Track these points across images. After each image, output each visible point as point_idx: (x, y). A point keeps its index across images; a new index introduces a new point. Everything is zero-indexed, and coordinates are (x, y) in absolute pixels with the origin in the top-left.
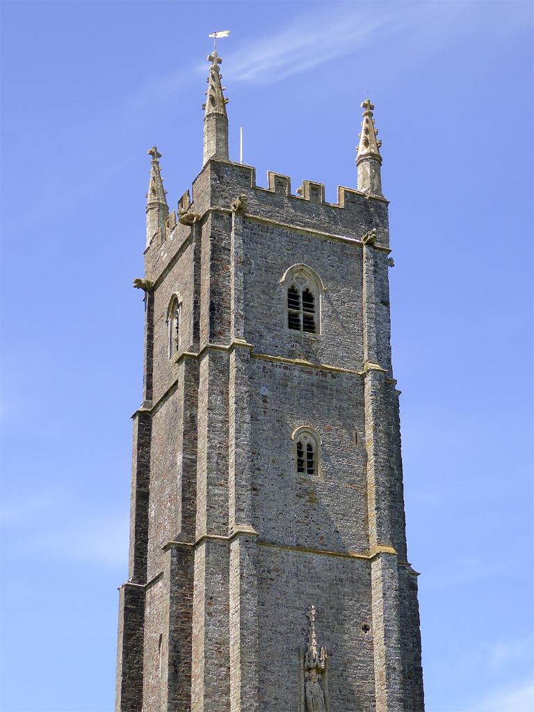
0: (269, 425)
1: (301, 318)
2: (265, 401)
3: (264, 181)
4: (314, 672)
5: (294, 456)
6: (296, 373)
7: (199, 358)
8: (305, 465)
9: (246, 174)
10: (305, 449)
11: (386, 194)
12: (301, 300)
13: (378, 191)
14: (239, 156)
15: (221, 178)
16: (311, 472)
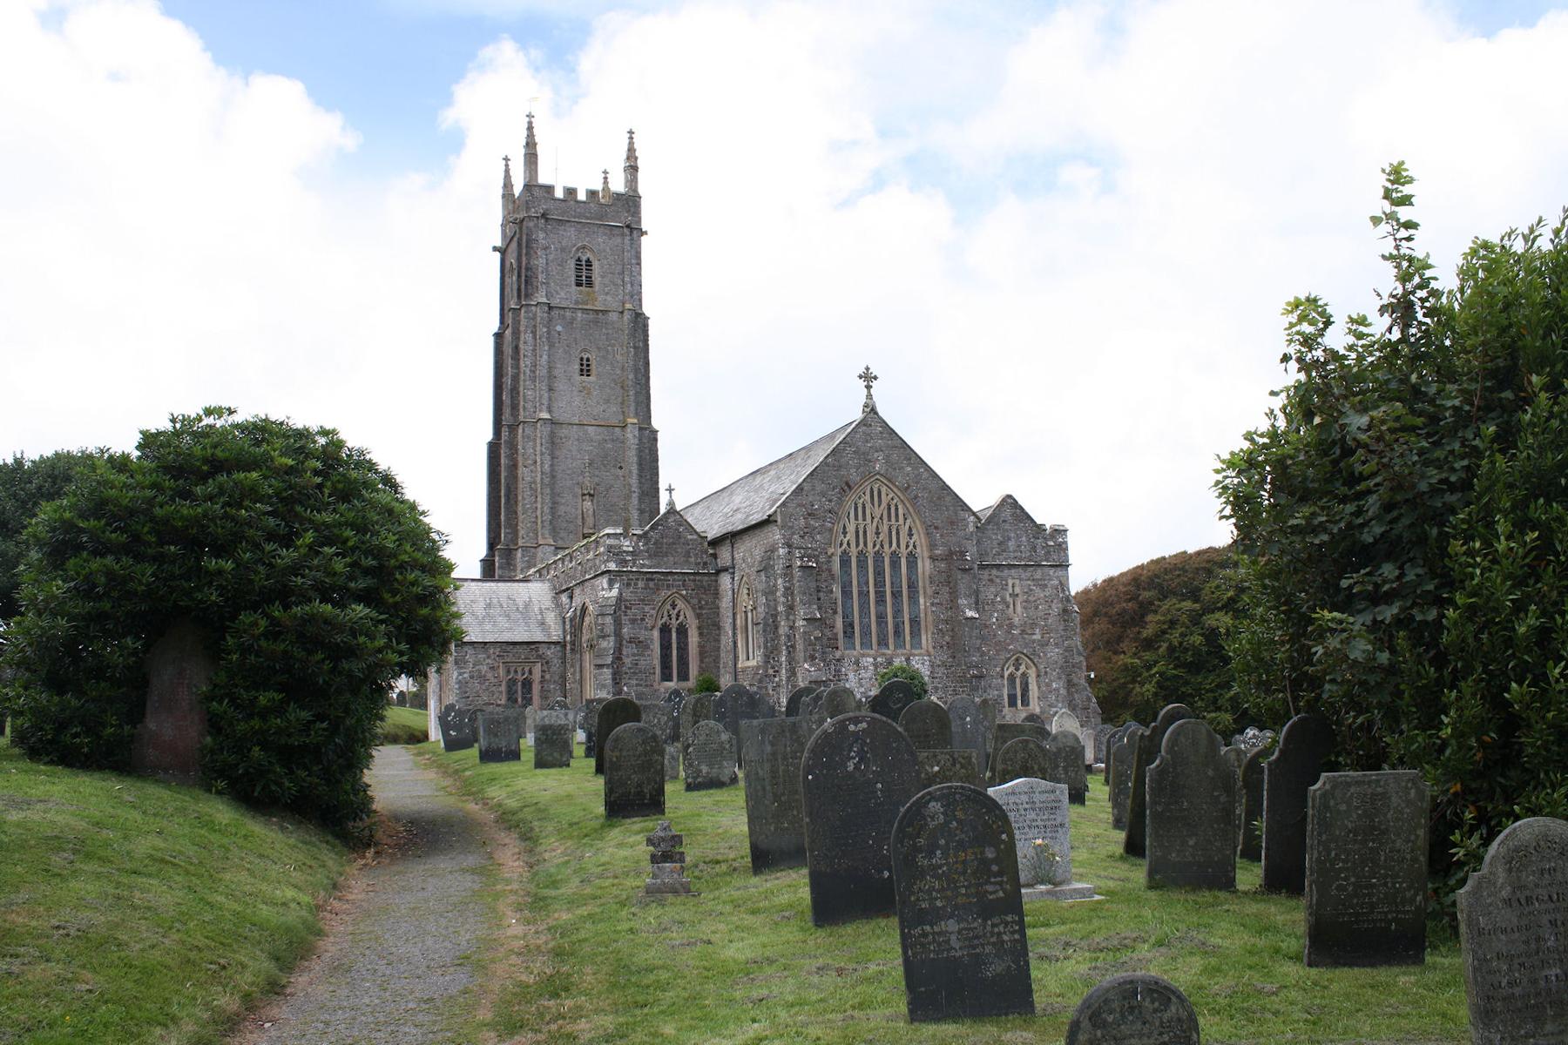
1: (584, 278)
3: (559, 194)
4: (587, 497)
5: (577, 367)
6: (580, 315)
7: (520, 309)
8: (585, 373)
9: (549, 189)
10: (585, 362)
11: (641, 190)
12: (584, 267)
13: (635, 190)
14: (543, 179)
15: (532, 195)
16: (588, 375)
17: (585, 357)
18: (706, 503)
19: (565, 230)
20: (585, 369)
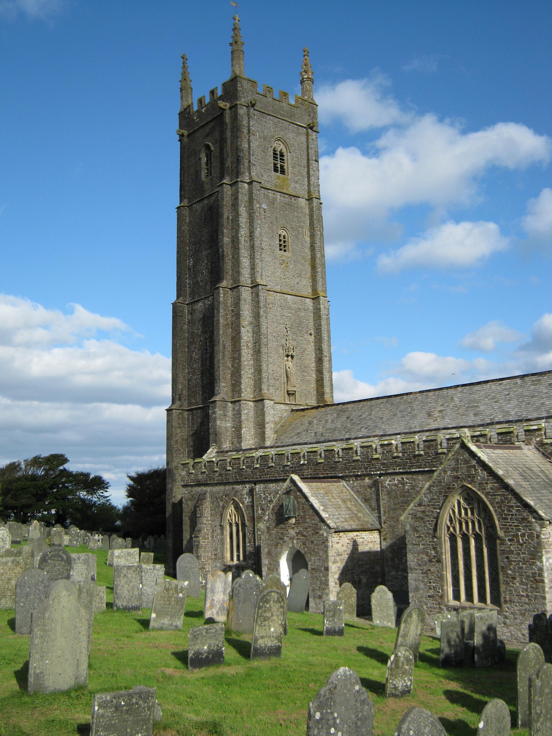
0: (267, 225)
1: (279, 167)
2: (265, 212)
6: (279, 197)
8: (282, 247)
17: (283, 234)
18: (534, 378)
19: (266, 122)
20: (283, 246)
